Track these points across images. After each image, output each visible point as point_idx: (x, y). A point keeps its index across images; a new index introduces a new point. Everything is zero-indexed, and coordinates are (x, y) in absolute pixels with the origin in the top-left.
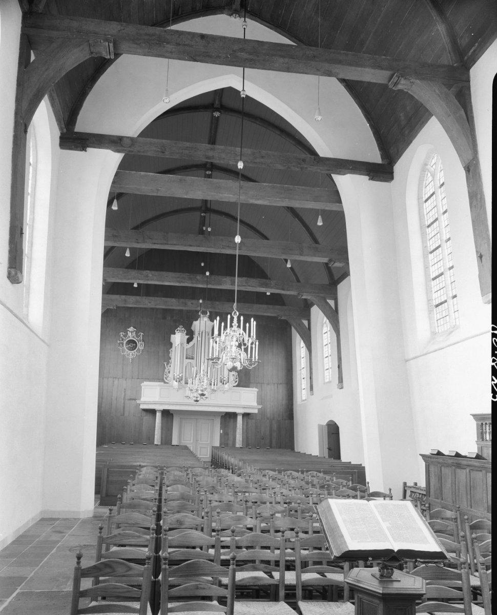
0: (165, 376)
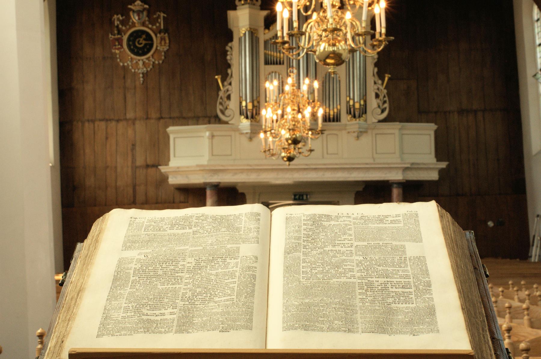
0: (219, 107)
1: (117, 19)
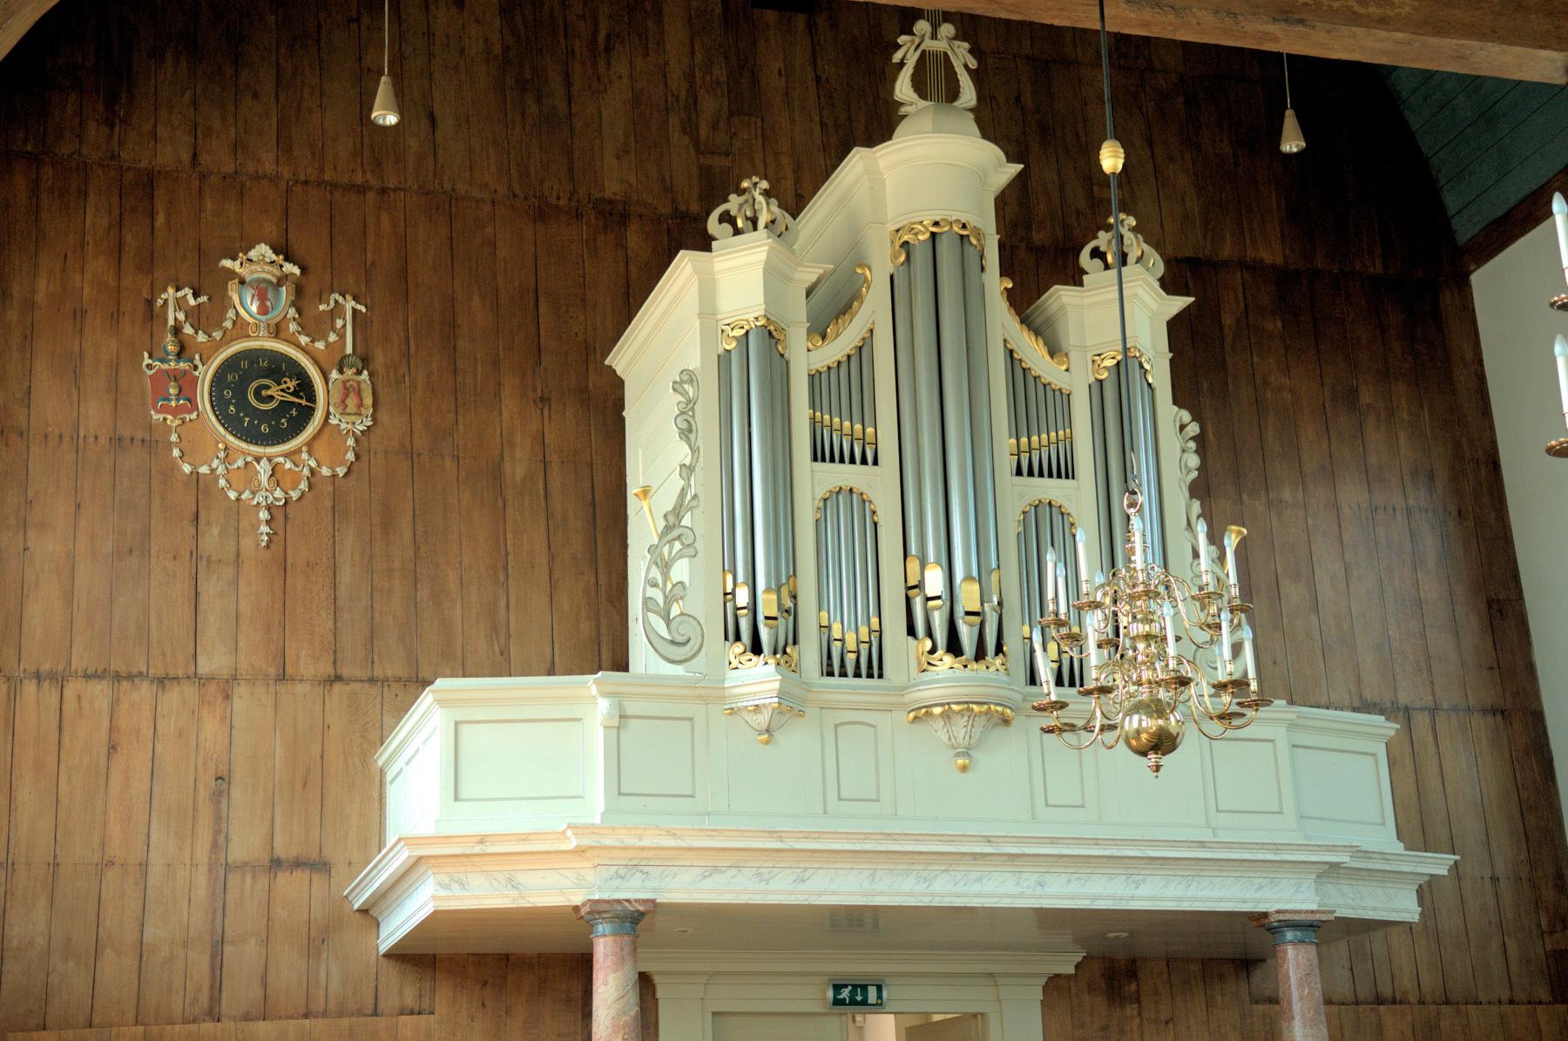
1: (175, 302)
